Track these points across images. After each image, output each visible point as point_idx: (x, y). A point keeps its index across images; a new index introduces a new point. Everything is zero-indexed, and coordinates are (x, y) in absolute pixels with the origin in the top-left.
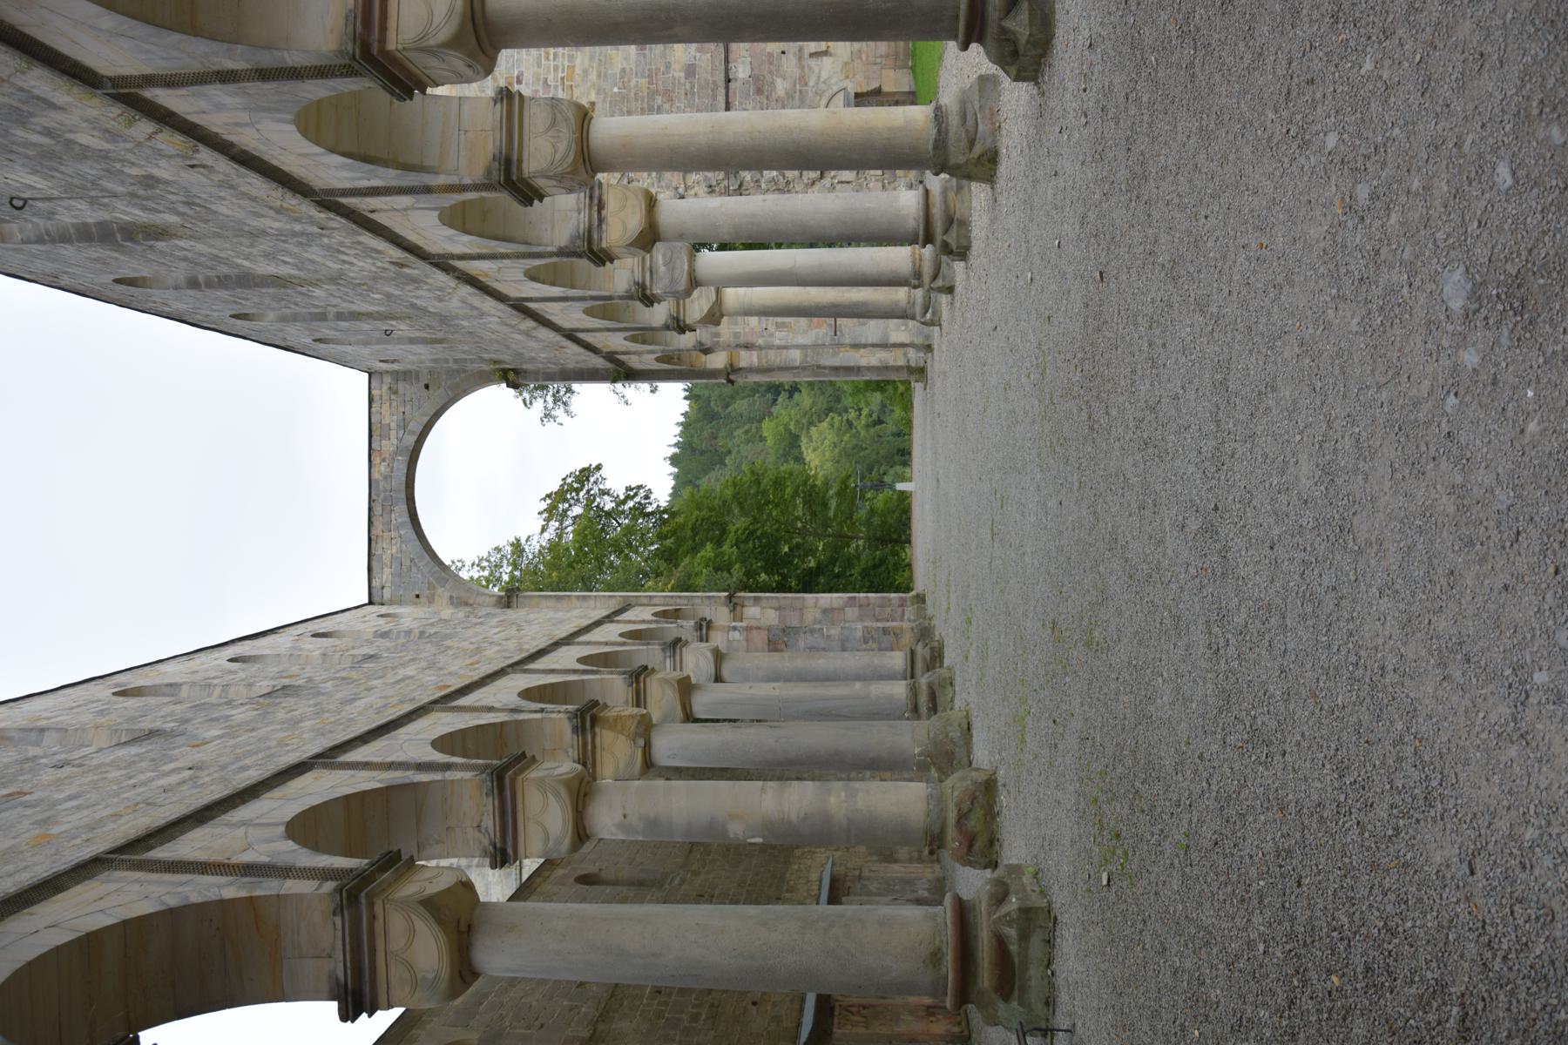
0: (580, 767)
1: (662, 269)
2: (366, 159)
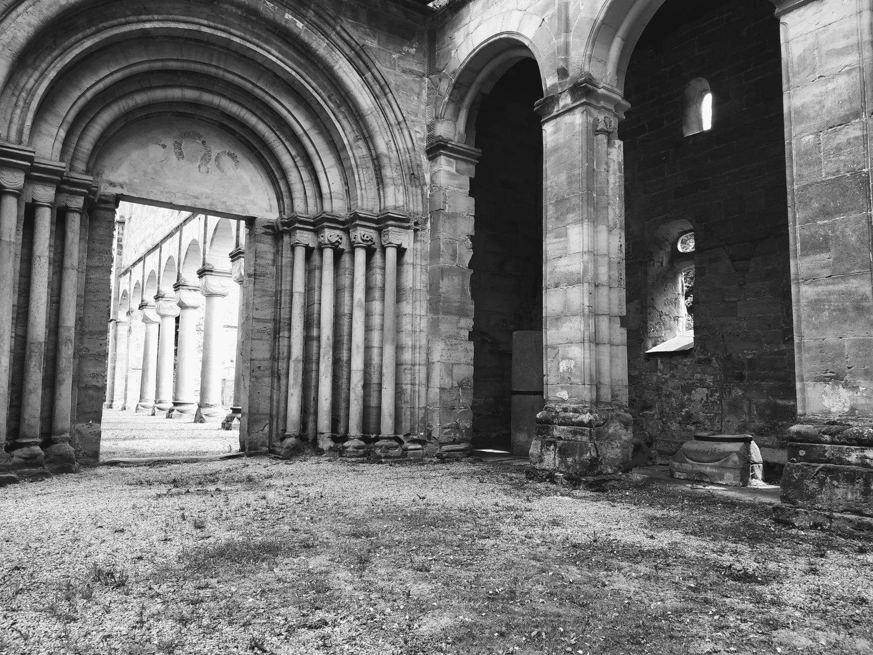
2: (216, 229)
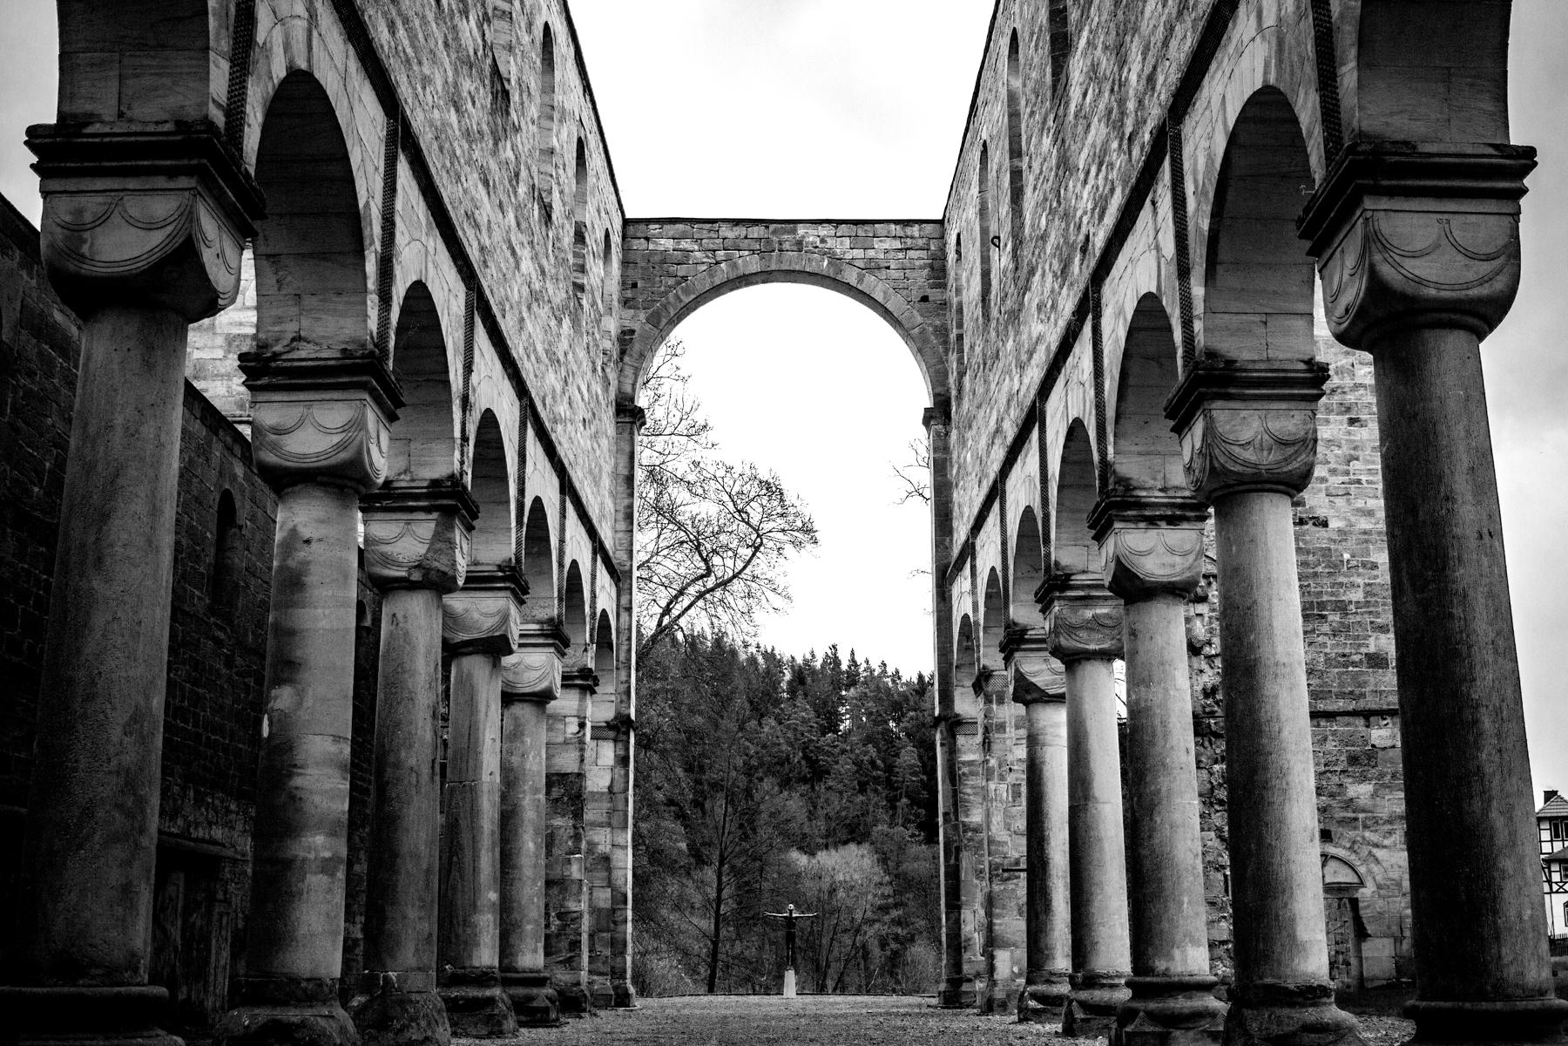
0: (380, 481)
1: (1089, 614)
